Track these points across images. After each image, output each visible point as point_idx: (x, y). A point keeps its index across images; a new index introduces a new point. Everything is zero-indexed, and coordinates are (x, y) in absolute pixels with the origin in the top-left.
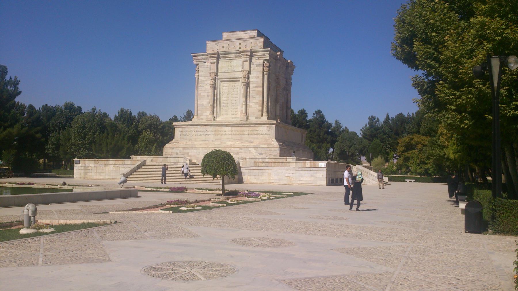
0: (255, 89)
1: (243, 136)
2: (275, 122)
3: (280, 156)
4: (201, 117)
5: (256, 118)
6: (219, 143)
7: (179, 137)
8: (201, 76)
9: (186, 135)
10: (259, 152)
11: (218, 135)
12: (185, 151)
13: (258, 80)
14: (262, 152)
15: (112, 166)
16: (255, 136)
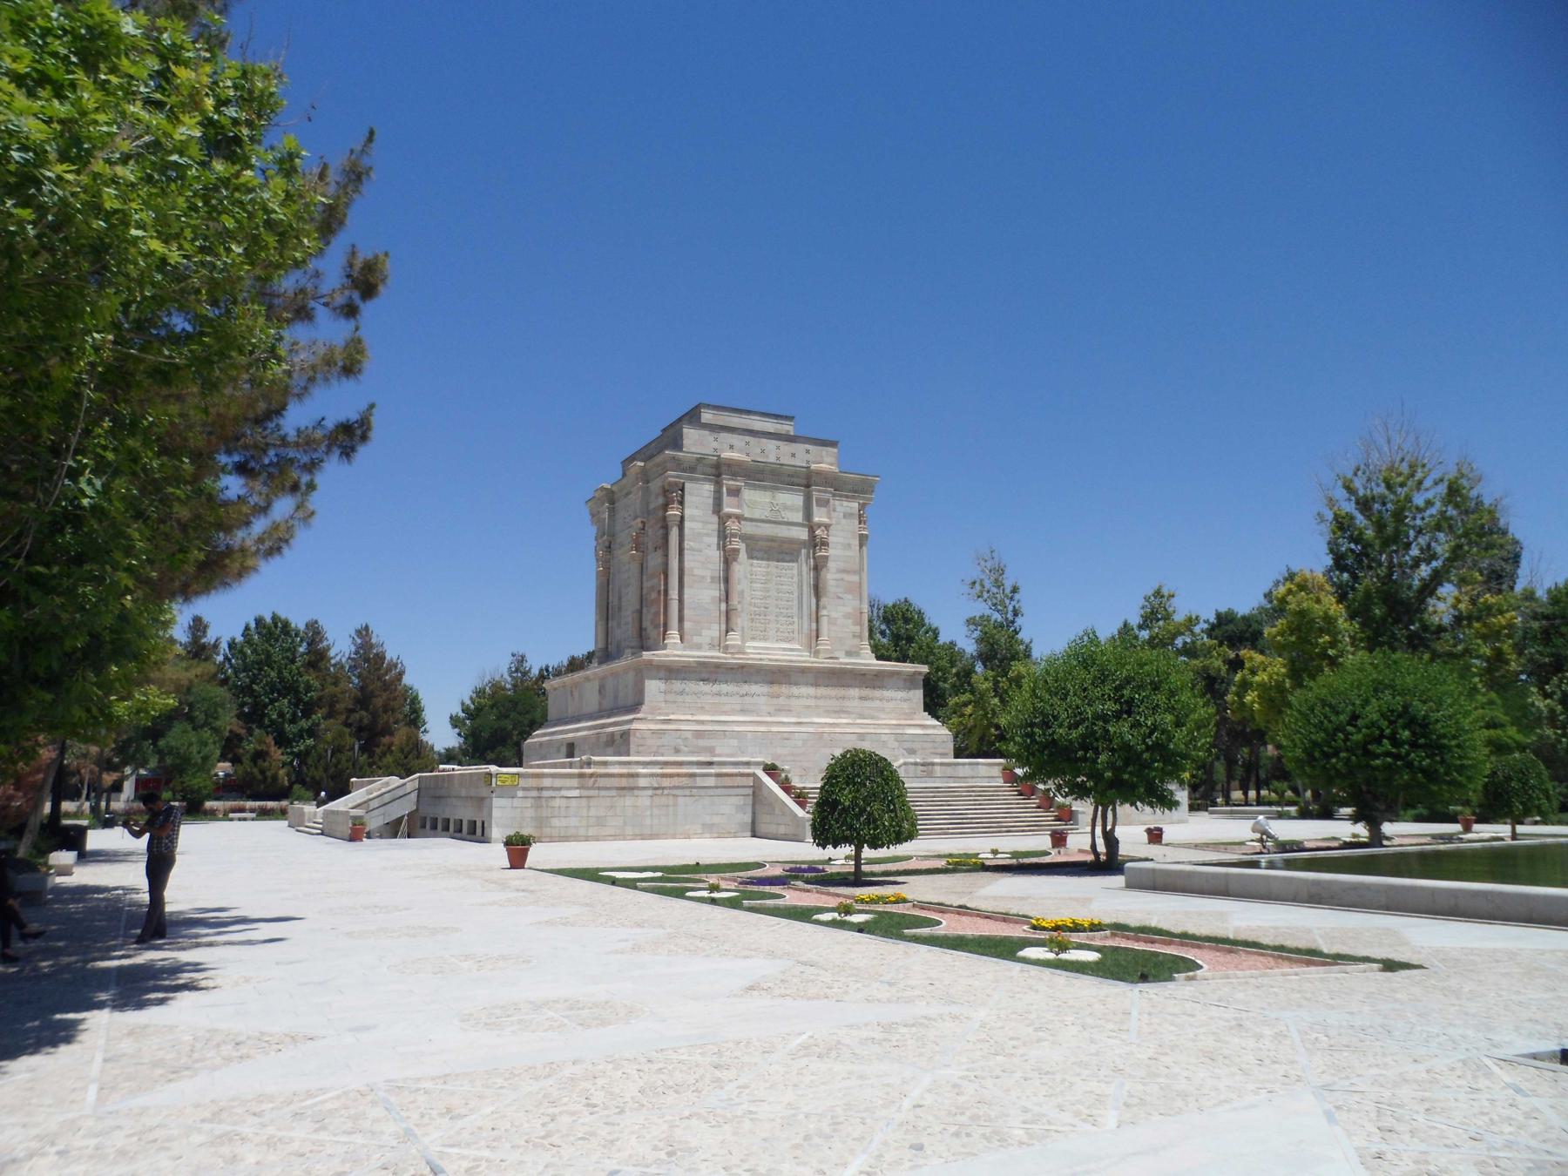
0: (839, 576)
1: (847, 703)
2: (925, 669)
3: (956, 756)
4: (696, 639)
5: (849, 654)
6: (793, 720)
7: (661, 697)
8: (693, 519)
9: (681, 693)
10: (907, 745)
11: (778, 697)
12: (701, 743)
13: (848, 553)
14: (914, 746)
15: (650, 792)
16: (877, 704)
